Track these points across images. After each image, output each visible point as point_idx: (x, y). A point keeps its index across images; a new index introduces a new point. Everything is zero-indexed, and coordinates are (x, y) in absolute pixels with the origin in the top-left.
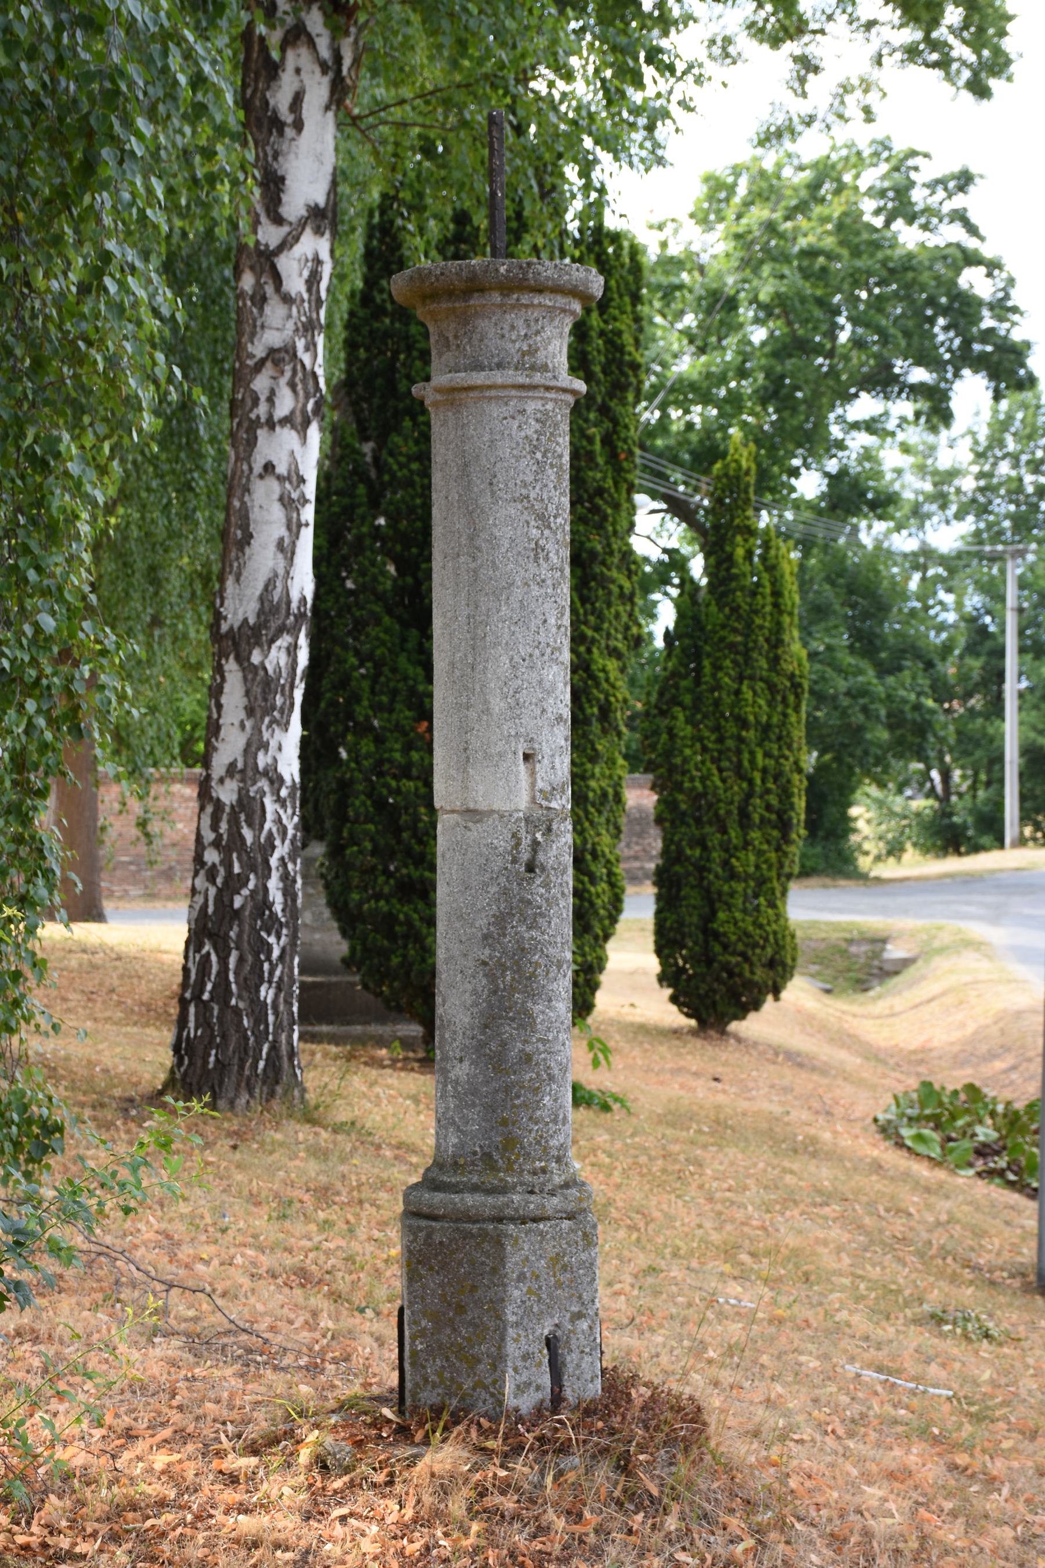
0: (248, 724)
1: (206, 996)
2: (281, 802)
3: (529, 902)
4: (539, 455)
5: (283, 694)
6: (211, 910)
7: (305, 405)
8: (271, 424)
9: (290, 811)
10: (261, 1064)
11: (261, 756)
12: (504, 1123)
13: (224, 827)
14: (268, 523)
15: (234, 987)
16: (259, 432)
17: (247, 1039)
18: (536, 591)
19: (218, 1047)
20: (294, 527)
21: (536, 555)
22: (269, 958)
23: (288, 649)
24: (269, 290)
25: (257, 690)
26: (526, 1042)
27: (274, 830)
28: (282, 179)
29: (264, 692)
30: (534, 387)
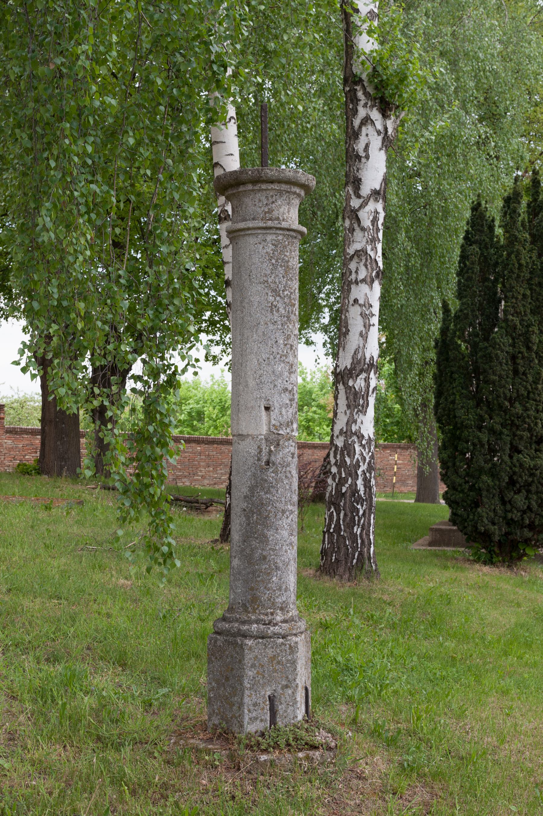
0: (348, 412)
1: (332, 530)
2: (363, 447)
3: (266, 481)
4: (273, 261)
5: (363, 399)
6: (333, 493)
7: (371, 274)
8: (357, 283)
9: (367, 450)
10: (355, 561)
11: (353, 425)
12: (252, 589)
13: (338, 457)
14: (356, 325)
15: (342, 526)
16: (352, 286)
17: (348, 549)
18: (271, 327)
19: (336, 552)
20: (368, 326)
21: (272, 309)
22: (357, 515)
23: (365, 379)
24: (356, 226)
25: (351, 397)
26: (263, 549)
27: (360, 458)
28: (360, 179)
29: (354, 398)
30: (270, 228)
